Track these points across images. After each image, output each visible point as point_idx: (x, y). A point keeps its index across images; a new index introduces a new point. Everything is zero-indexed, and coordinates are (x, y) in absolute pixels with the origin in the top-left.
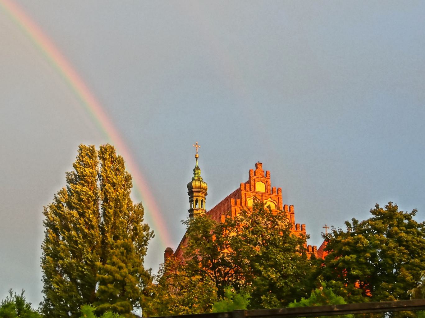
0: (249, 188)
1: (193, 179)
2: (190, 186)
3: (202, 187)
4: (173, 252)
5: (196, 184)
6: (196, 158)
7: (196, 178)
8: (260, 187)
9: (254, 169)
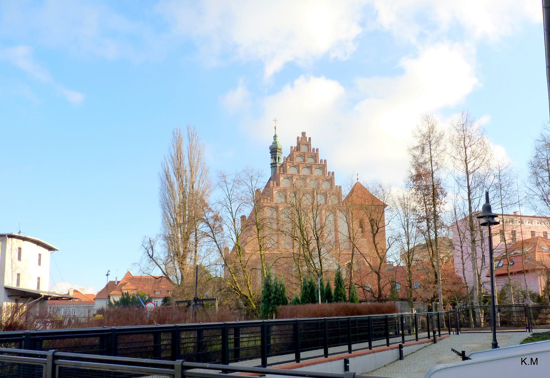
1: (273, 143)
3: (278, 148)
6: (275, 128)
8: (304, 149)
9: (300, 136)
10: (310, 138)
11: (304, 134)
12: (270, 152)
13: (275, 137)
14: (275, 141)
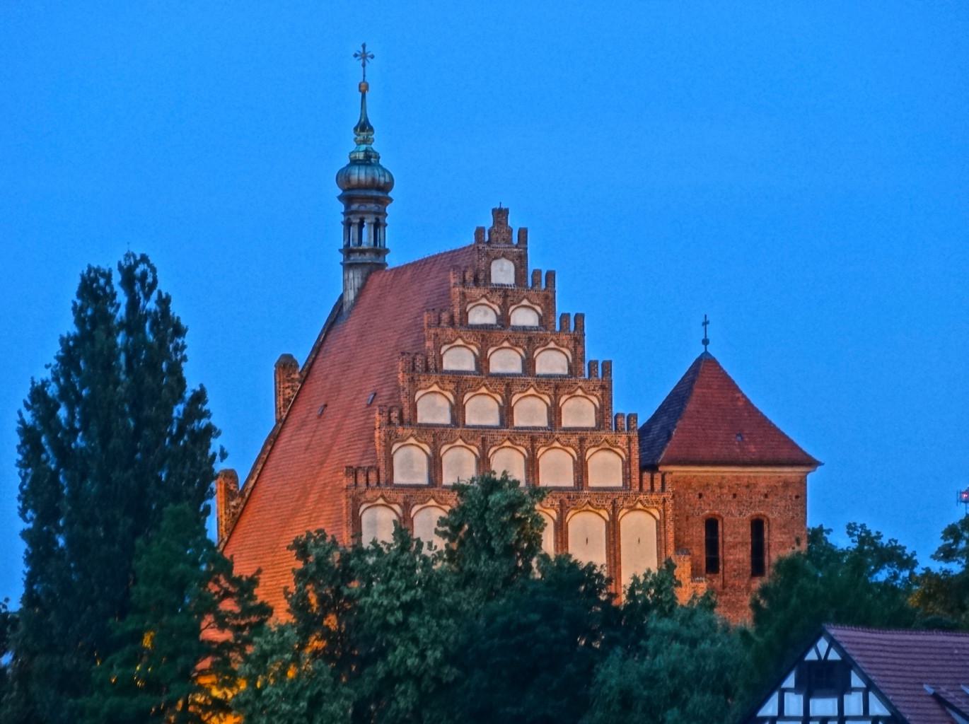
0: (472, 279)
1: (354, 162)
2: (343, 178)
4: (297, 366)
5: (359, 175)
6: (364, 89)
7: (361, 156)
8: (503, 273)
9: (488, 223)
10: (523, 233)
11: (500, 214)
12: (340, 198)
13: (364, 126)
14: (363, 147)
